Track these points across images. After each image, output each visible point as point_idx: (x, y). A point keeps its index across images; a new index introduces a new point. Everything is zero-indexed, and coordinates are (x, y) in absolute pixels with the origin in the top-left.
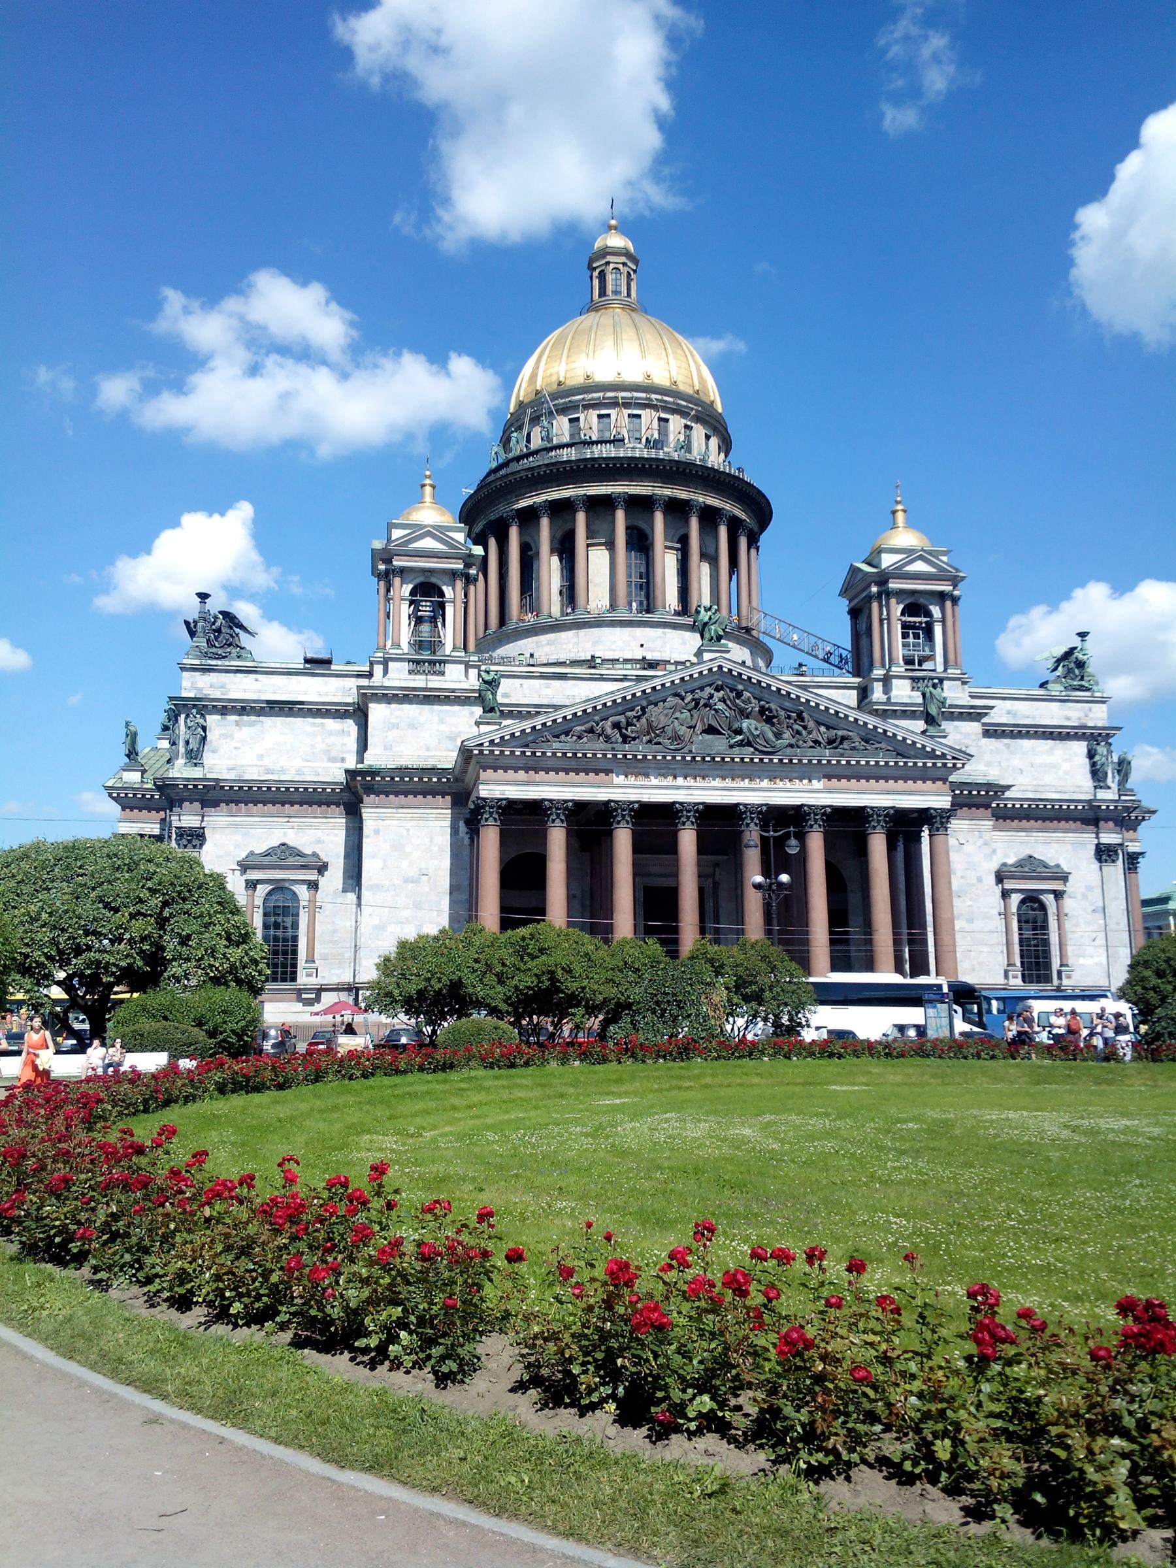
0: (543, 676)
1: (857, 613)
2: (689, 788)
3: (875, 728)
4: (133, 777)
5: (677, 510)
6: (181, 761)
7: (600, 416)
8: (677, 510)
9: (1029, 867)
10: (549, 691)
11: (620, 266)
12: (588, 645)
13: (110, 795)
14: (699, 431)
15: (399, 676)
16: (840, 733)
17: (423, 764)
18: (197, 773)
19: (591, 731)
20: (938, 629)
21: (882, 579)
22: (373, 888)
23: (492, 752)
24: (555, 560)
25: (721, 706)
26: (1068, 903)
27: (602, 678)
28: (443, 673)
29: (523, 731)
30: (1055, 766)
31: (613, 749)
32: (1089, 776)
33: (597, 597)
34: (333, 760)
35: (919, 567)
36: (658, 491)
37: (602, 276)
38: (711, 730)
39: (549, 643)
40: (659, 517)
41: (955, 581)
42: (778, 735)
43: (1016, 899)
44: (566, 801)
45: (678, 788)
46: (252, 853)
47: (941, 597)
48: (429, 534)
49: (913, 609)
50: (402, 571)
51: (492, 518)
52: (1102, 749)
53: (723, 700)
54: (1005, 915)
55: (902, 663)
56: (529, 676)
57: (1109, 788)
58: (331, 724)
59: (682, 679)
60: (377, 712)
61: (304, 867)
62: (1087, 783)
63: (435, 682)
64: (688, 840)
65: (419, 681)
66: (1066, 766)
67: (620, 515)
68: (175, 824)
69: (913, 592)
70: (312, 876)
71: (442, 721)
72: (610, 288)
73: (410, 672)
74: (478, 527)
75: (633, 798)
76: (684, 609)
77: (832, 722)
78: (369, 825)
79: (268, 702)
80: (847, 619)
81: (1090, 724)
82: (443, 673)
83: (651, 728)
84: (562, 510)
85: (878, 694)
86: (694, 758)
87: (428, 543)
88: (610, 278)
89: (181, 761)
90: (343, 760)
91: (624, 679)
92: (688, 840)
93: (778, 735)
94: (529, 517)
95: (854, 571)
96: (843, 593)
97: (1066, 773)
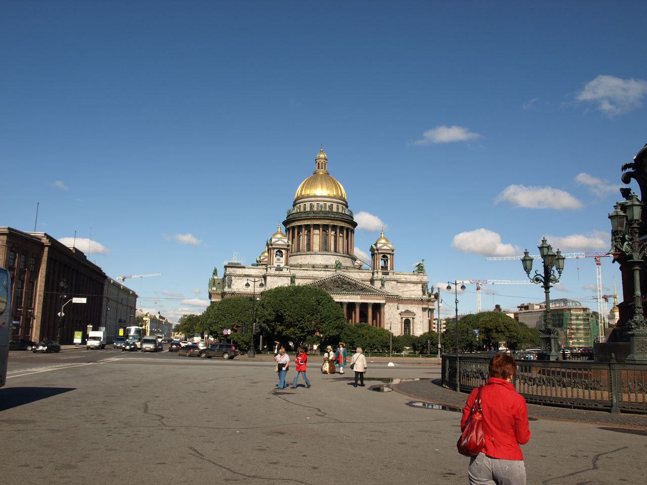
0: (303, 270)
1: (373, 255)
5: (334, 228)
6: (227, 287)
8: (334, 228)
9: (407, 312)
10: (304, 273)
14: (340, 206)
18: (230, 290)
20: (389, 261)
21: (377, 250)
25: (340, 282)
26: (415, 320)
27: (316, 270)
28: (282, 270)
33: (316, 247)
35: (385, 247)
37: (319, 163)
38: (337, 287)
39: (304, 258)
40: (330, 229)
41: (393, 251)
42: (351, 288)
43: (404, 319)
47: (390, 254)
49: (384, 256)
51: (291, 226)
52: (425, 287)
54: (402, 323)
56: (300, 270)
60: (269, 279)
62: (421, 293)
67: (321, 229)
72: (320, 167)
73: (276, 270)
74: (288, 227)
76: (335, 251)
82: (282, 270)
83: (326, 286)
84: (308, 227)
85: (376, 275)
87: (280, 242)
88: (320, 165)
89: (227, 287)
91: (321, 270)
93: (351, 288)
94: (300, 227)
95: (372, 247)
96: (370, 250)
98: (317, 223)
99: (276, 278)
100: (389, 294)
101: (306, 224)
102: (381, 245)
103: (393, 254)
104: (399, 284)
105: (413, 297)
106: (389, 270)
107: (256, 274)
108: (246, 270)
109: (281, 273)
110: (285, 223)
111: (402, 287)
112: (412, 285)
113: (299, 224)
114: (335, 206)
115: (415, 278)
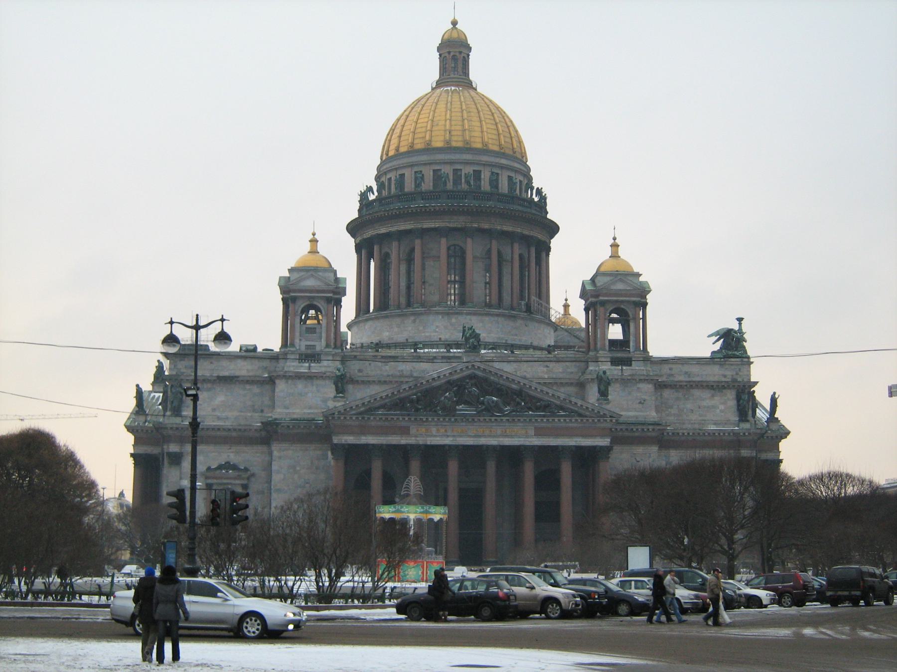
1: (587, 310)
2: (454, 436)
3: (565, 399)
4: (142, 419)
7: (434, 171)
10: (387, 368)
11: (457, 54)
12: (421, 328)
13: (128, 430)
15: (292, 366)
16: (543, 403)
17: (306, 417)
19: (396, 404)
20: (632, 325)
22: (279, 491)
23: (339, 418)
24: (403, 268)
29: (357, 406)
30: (714, 407)
31: (409, 415)
32: (737, 413)
34: (254, 411)
35: (620, 286)
36: (469, 225)
41: (643, 291)
44: (382, 445)
45: (448, 436)
46: (209, 469)
48: (312, 276)
50: (294, 300)
53: (476, 385)
55: (607, 348)
57: (748, 421)
58: (256, 389)
59: (450, 373)
60: (281, 386)
61: (239, 477)
63: (316, 368)
64: (453, 467)
65: (304, 368)
66: (722, 407)
68: (166, 451)
69: (617, 301)
70: (245, 482)
71: (318, 391)
74: (358, 241)
75: (421, 443)
77: (539, 396)
78: (275, 453)
79: (218, 377)
80: (584, 313)
81: (739, 379)
86: (456, 420)
87: (310, 283)
89: (168, 413)
90: (262, 411)
92: (453, 467)
96: (582, 297)
97: (722, 411)
98: (433, 226)
99: (300, 386)
100: (621, 420)
101: (402, 228)
102: (607, 279)
103: (644, 305)
104: (667, 393)
105: (713, 427)
106: (632, 349)
107: (251, 374)
108: (225, 363)
109: (316, 368)
110: (353, 228)
111: (678, 399)
112: (706, 394)
113: (383, 230)
114: (486, 175)
115: (715, 373)
